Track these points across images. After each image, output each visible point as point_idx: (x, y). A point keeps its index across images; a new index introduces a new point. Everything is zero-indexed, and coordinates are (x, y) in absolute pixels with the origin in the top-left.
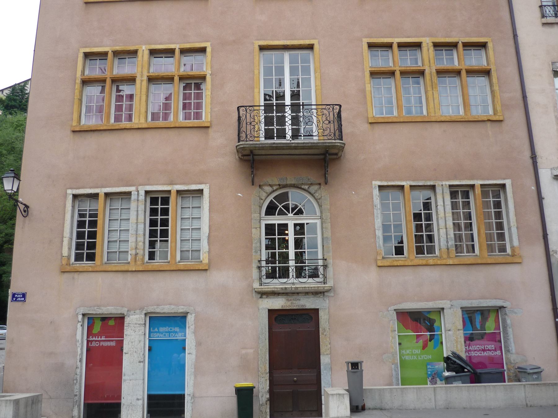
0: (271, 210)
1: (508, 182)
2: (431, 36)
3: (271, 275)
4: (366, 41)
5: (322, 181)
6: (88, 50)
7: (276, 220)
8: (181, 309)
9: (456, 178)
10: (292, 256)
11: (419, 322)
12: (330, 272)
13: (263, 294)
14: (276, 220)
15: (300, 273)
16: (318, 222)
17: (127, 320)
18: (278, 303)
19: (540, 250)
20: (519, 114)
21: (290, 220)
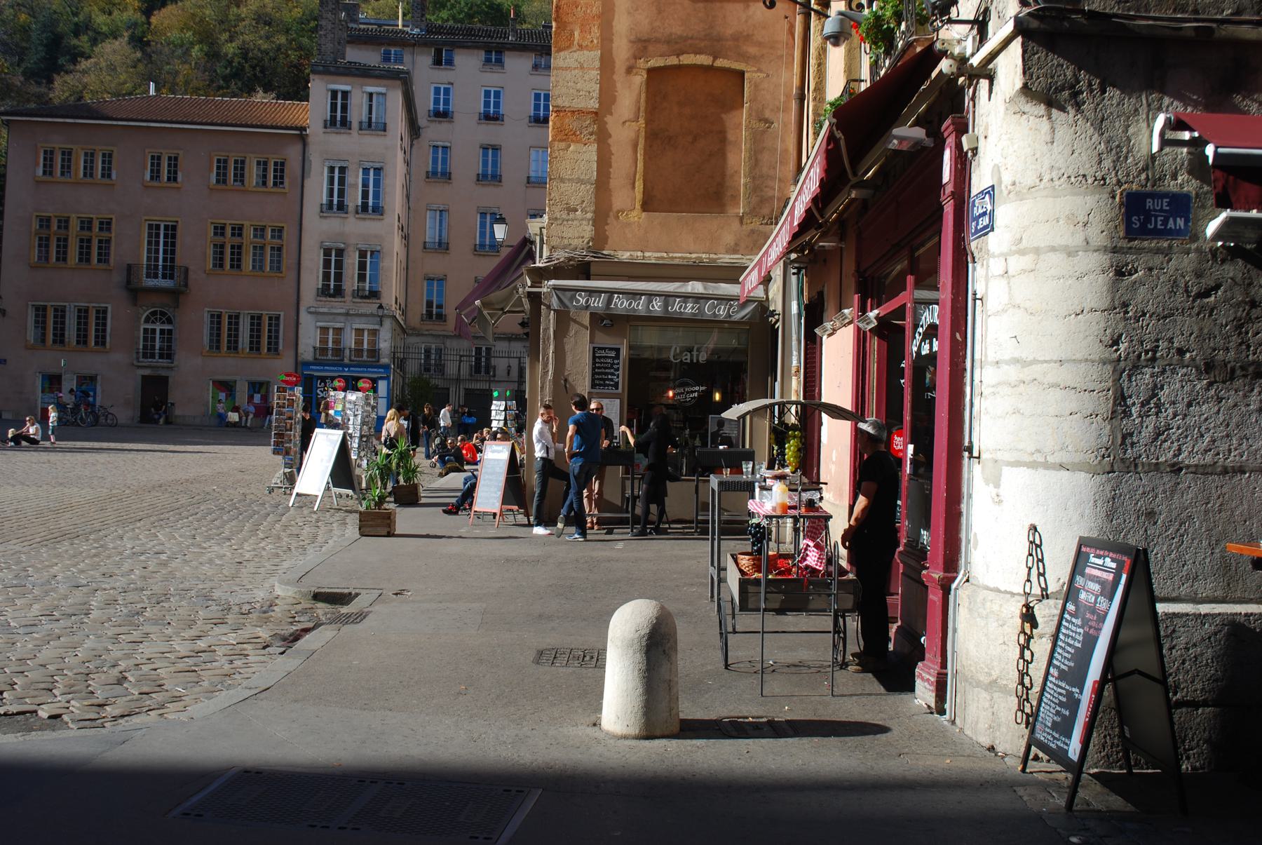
0: (147, 320)
1: (282, 314)
3: (145, 356)
7: (150, 326)
8: (94, 372)
11: (226, 387)
12: (176, 357)
13: (139, 367)
14: (150, 326)
15: (161, 356)
18: (147, 372)
19: (292, 353)
20: (293, 275)
21: (158, 327)
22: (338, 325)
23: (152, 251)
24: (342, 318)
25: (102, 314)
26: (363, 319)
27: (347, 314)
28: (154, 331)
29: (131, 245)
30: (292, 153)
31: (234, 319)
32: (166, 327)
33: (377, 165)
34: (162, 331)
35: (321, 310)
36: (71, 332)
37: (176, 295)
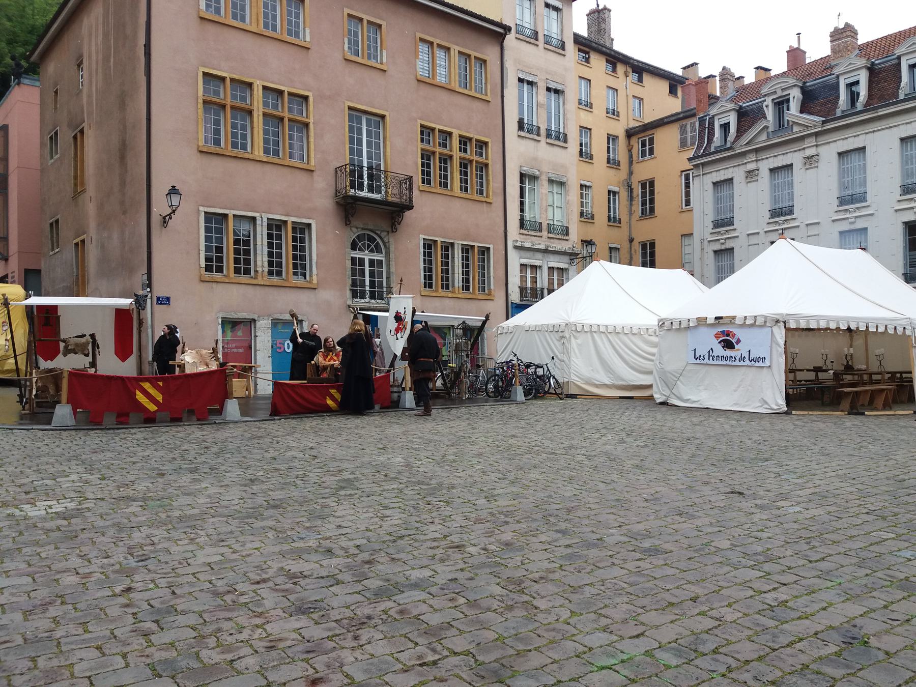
0: (354, 246)
1: (491, 246)
2: (459, 129)
4: (419, 122)
5: (390, 230)
6: (207, 70)
7: (357, 255)
9: (465, 240)
10: (367, 283)
14: (357, 255)
16: (383, 259)
17: (258, 324)
21: (367, 256)
22: (537, 263)
23: (355, 151)
24: (539, 255)
25: (302, 230)
26: (557, 257)
27: (546, 251)
28: (362, 261)
29: (328, 144)
30: (490, 53)
31: (448, 247)
32: (376, 257)
33: (559, 87)
34: (372, 262)
35: (528, 245)
36: (261, 259)
37: (394, 213)
